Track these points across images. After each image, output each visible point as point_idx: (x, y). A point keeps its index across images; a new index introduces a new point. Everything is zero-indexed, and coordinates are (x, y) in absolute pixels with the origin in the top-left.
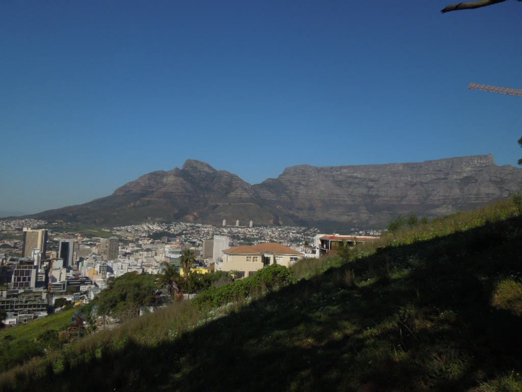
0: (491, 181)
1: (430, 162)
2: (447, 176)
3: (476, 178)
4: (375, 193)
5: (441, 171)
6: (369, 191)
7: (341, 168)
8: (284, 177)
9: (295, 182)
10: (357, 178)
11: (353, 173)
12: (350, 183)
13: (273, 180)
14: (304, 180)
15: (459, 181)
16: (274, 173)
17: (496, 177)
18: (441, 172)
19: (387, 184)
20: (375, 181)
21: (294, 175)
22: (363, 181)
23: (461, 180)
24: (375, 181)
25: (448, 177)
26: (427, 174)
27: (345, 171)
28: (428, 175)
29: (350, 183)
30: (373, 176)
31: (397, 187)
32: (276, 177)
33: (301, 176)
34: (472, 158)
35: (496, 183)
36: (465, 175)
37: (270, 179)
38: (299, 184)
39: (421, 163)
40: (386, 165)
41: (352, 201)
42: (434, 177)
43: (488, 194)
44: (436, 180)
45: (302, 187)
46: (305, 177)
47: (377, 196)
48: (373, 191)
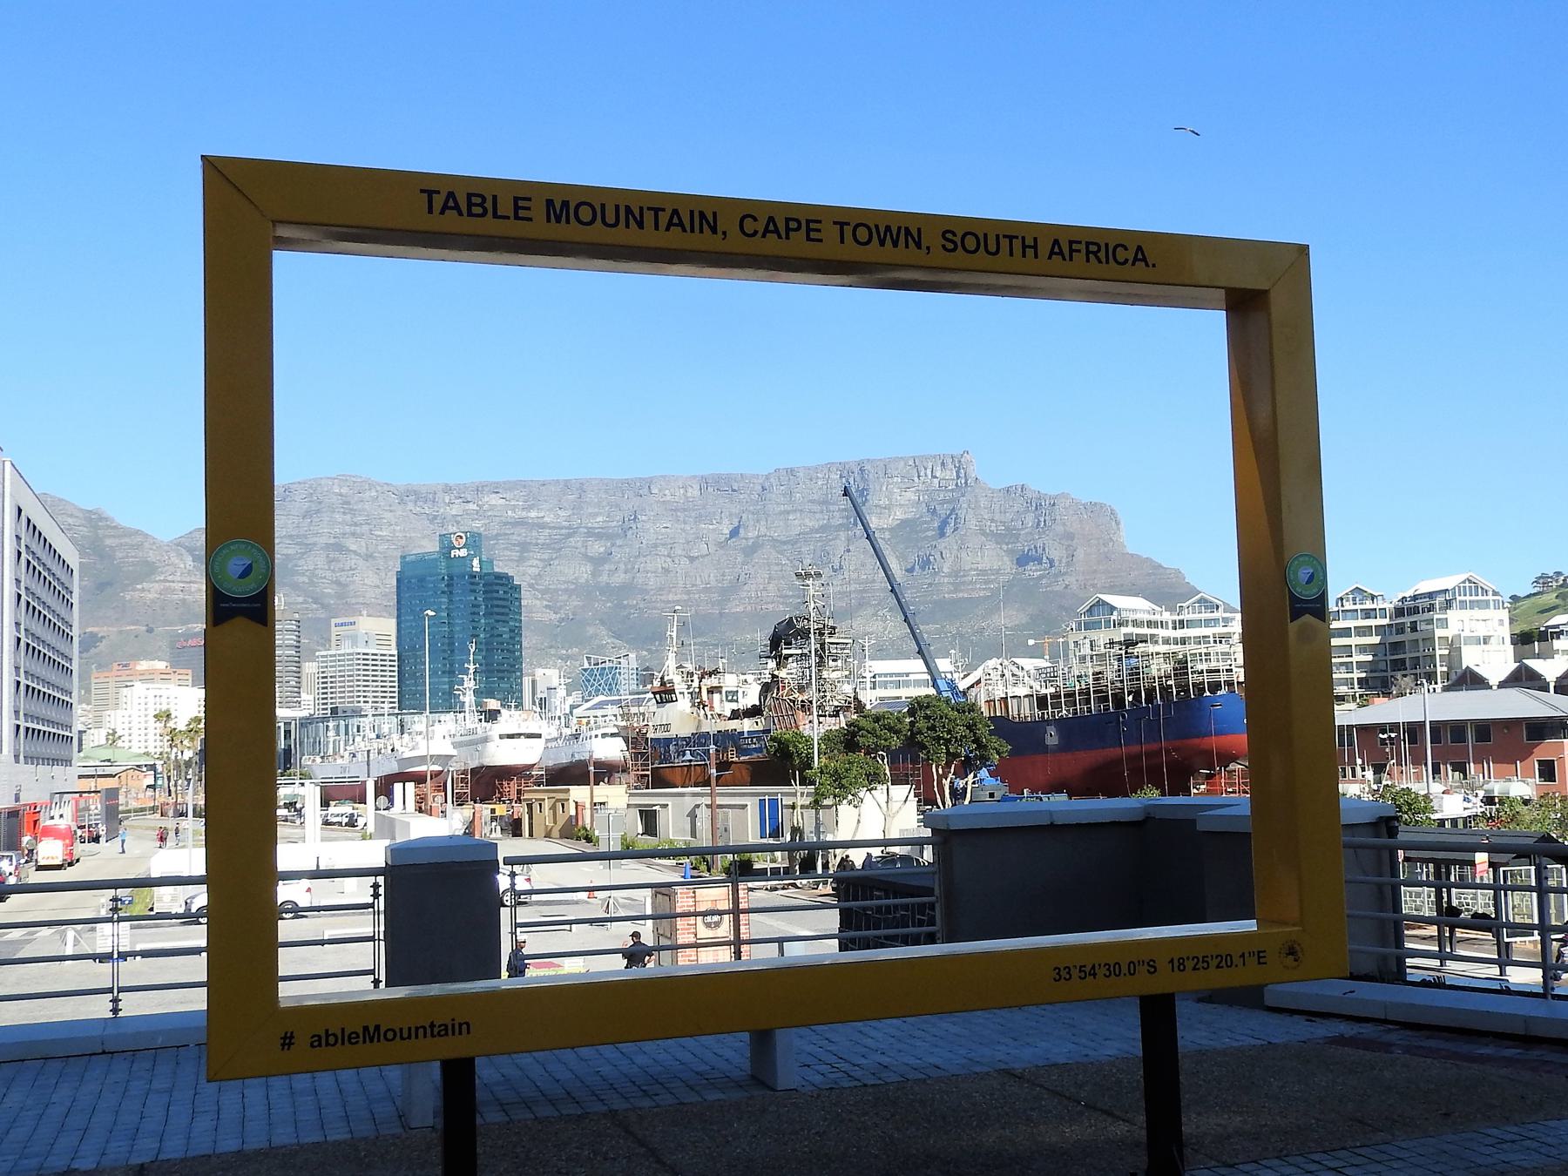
0: (984, 533)
1: (791, 472)
4: (619, 578)
6: (594, 574)
7: (479, 489)
9: (323, 540)
10: (543, 526)
11: (530, 508)
12: (524, 547)
14: (353, 534)
17: (992, 520)
19: (655, 546)
20: (609, 537)
21: (306, 514)
22: (569, 536)
23: (891, 530)
24: (609, 537)
27: (495, 500)
29: (524, 547)
31: (692, 559)
33: (339, 517)
34: (917, 464)
35: (998, 538)
36: (899, 515)
38: (339, 548)
39: (767, 477)
40: (649, 483)
41: (547, 607)
42: (811, 523)
43: (983, 572)
44: (813, 531)
45: (353, 561)
47: (627, 589)
48: (611, 573)
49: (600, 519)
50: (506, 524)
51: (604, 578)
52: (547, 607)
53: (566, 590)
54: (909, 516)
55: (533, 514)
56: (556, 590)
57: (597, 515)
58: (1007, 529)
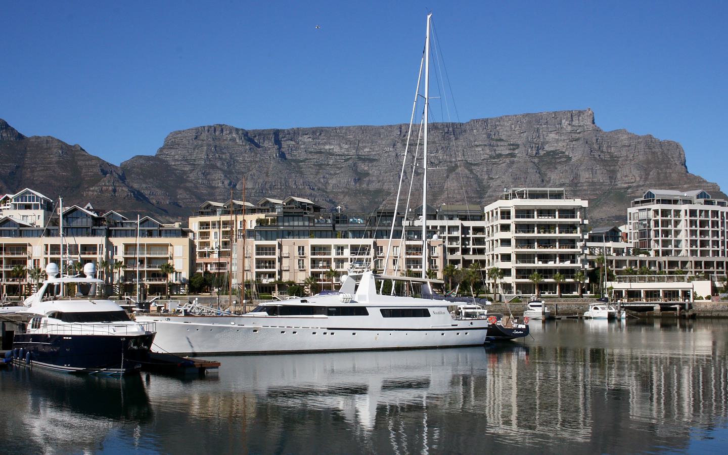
2: (514, 149)
3: (567, 153)
5: (501, 140)
8: (173, 152)
10: (330, 154)
13: (148, 158)
14: (220, 158)
15: (536, 160)
16: (150, 146)
18: (502, 143)
20: (371, 161)
24: (371, 161)
25: (516, 152)
26: (477, 146)
28: (480, 149)
30: (367, 150)
32: (153, 153)
36: (548, 148)
37: (141, 157)
46: (223, 153)
48: (369, 182)
49: (367, 150)
50: (311, 152)
51: (364, 186)
52: (331, 201)
53: (343, 192)
54: (552, 149)
55: (327, 147)
56: (337, 193)
57: (365, 147)
58: (612, 157)
